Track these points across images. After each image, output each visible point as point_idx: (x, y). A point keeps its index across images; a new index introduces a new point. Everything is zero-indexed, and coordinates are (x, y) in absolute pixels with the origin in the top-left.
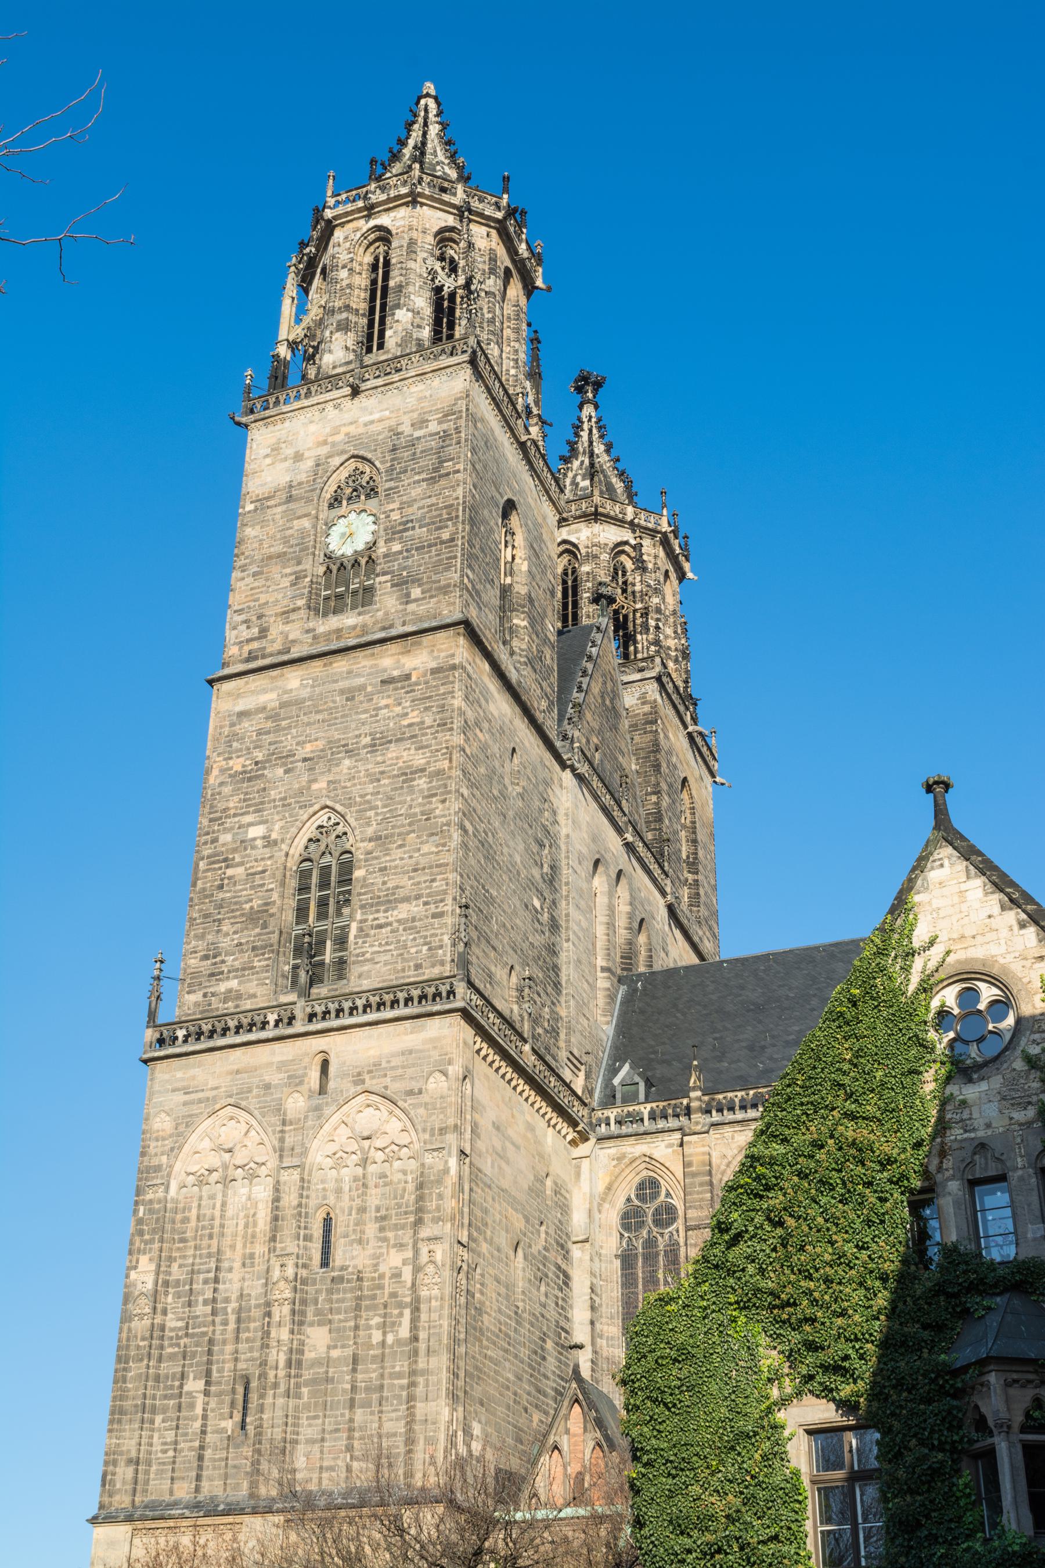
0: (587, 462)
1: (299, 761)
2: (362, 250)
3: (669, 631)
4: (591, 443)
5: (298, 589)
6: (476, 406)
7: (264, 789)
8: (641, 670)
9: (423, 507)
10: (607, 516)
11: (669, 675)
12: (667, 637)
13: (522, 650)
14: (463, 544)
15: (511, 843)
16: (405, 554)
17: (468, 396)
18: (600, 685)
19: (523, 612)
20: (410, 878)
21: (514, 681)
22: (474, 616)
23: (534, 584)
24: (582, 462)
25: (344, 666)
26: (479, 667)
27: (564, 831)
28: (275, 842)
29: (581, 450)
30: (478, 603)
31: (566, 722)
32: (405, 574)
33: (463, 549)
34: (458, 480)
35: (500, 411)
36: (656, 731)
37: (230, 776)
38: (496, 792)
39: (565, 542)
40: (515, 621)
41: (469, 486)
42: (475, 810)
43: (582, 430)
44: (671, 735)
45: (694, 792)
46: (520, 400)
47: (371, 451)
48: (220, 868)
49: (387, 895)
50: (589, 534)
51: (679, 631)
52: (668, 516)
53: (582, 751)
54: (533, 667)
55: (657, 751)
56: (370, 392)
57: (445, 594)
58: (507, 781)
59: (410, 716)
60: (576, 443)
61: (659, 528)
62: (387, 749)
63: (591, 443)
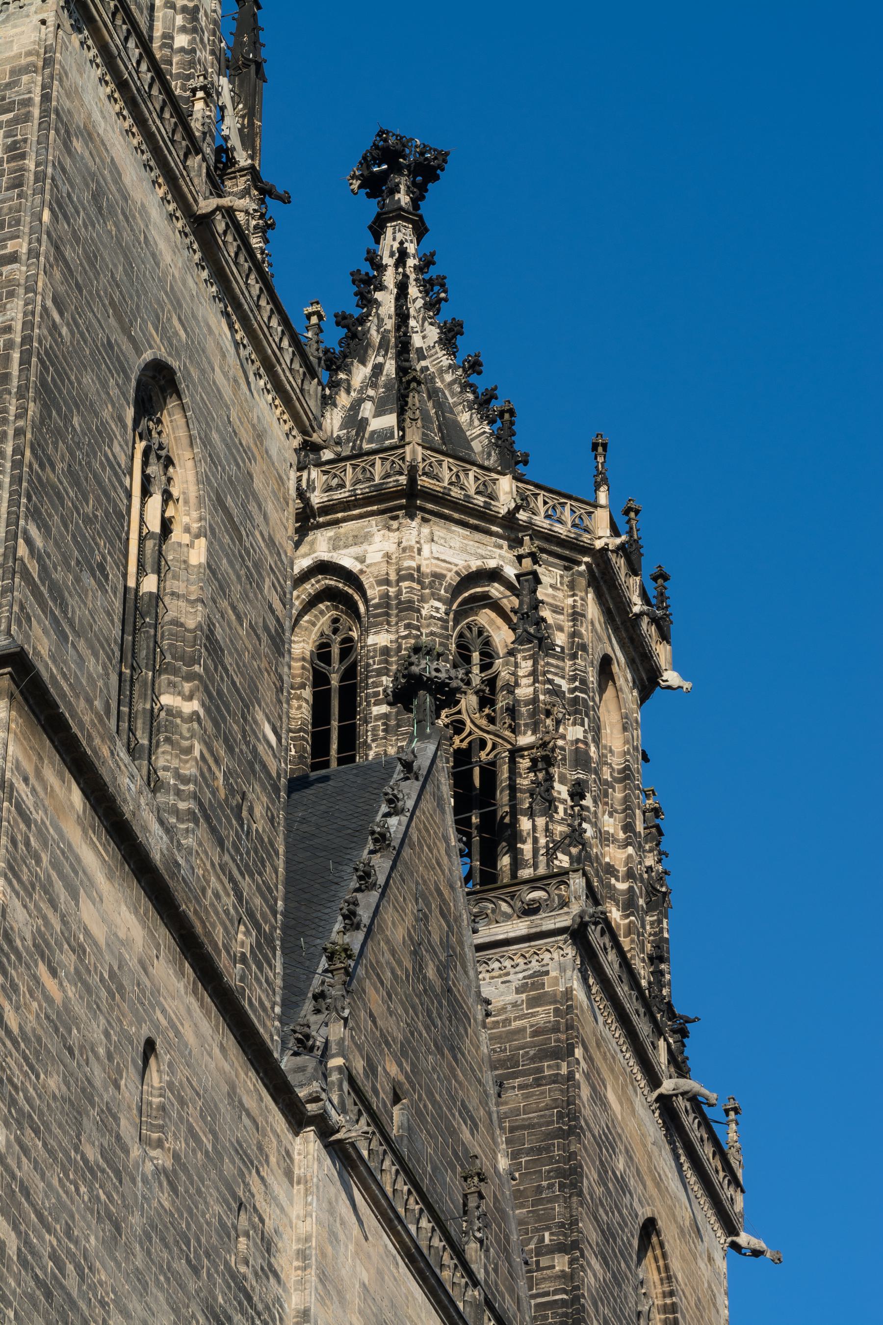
0: (390, 367)
3: (611, 824)
4: (402, 317)
6: (73, 93)
8: (531, 910)
10: (441, 499)
11: (609, 929)
12: (605, 838)
13: (185, 780)
14: (18, 450)
15: (134, 1305)
17: (48, 62)
18: (409, 920)
19: (189, 677)
21: (157, 856)
22: (44, 653)
23: (224, 604)
24: (378, 369)
26: (52, 794)
27: (294, 1302)
29: (375, 337)
30: (55, 621)
31: (309, 1006)
33: (17, 465)
34: (10, 282)
35: (141, 121)
36: (570, 1076)
38: (92, 1153)
39: (323, 568)
40: (166, 699)
41: (43, 299)
42: (26, 1192)
43: (381, 287)
44: (611, 1096)
45: (676, 1265)
46: (199, 106)
50: (391, 548)
51: (639, 827)
52: (611, 507)
53: (352, 1081)
54: (213, 830)
55: (571, 1131)
58: (127, 1129)
60: (362, 320)
61: (586, 538)
63: (402, 317)
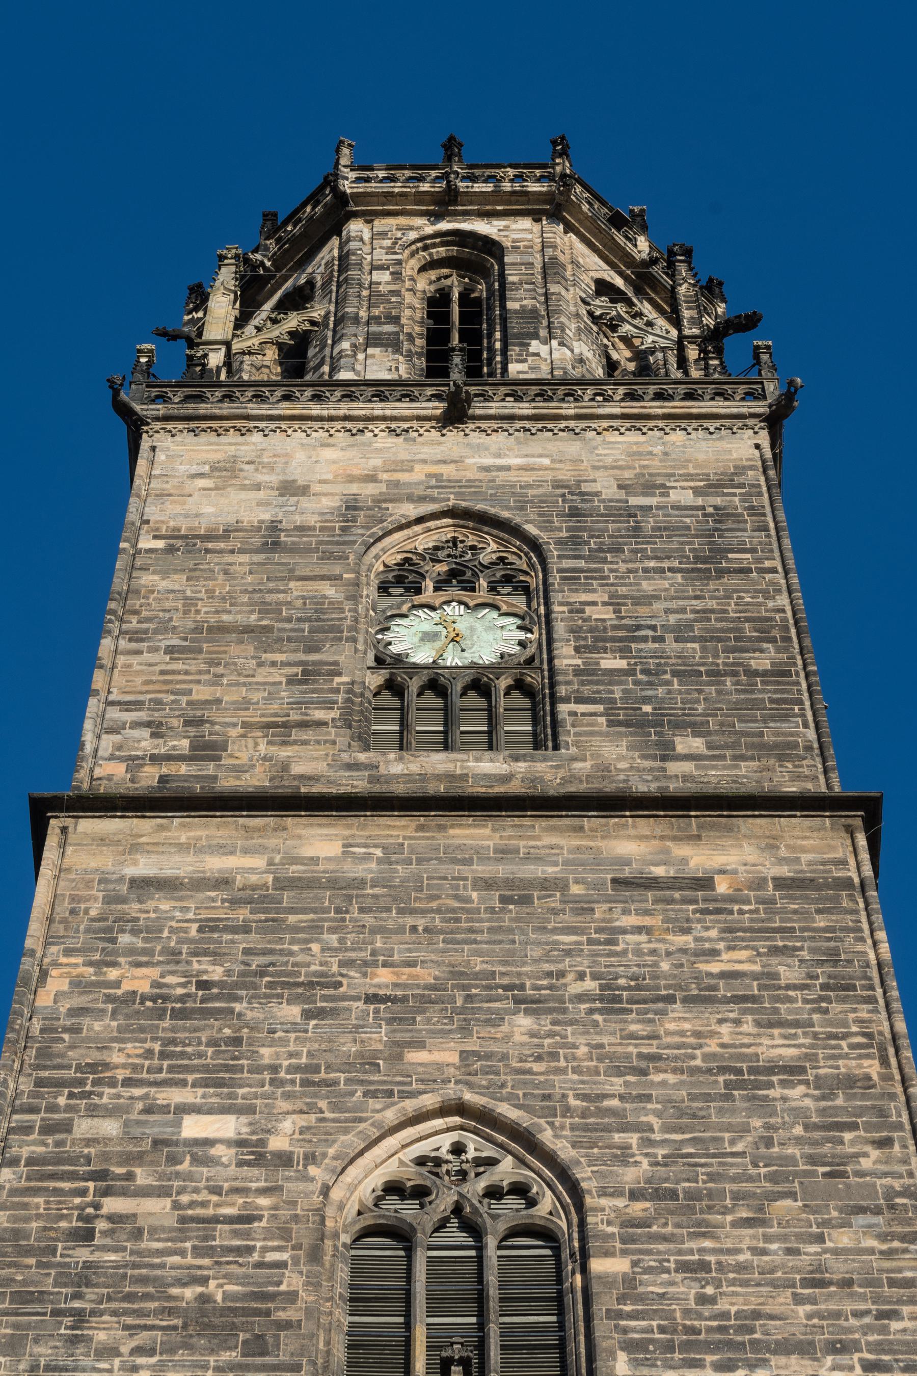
1: (356, 998)
2: (414, 264)
7: (237, 1041)
9: (683, 611)
20: (799, 1300)
25: (489, 838)
28: (285, 1159)
32: (647, 709)
37: (109, 999)
47: (508, 508)
48: (83, 1193)
49: (722, 1329)
56: (494, 425)
57: (781, 758)
59: (725, 956)
62: (664, 1013)
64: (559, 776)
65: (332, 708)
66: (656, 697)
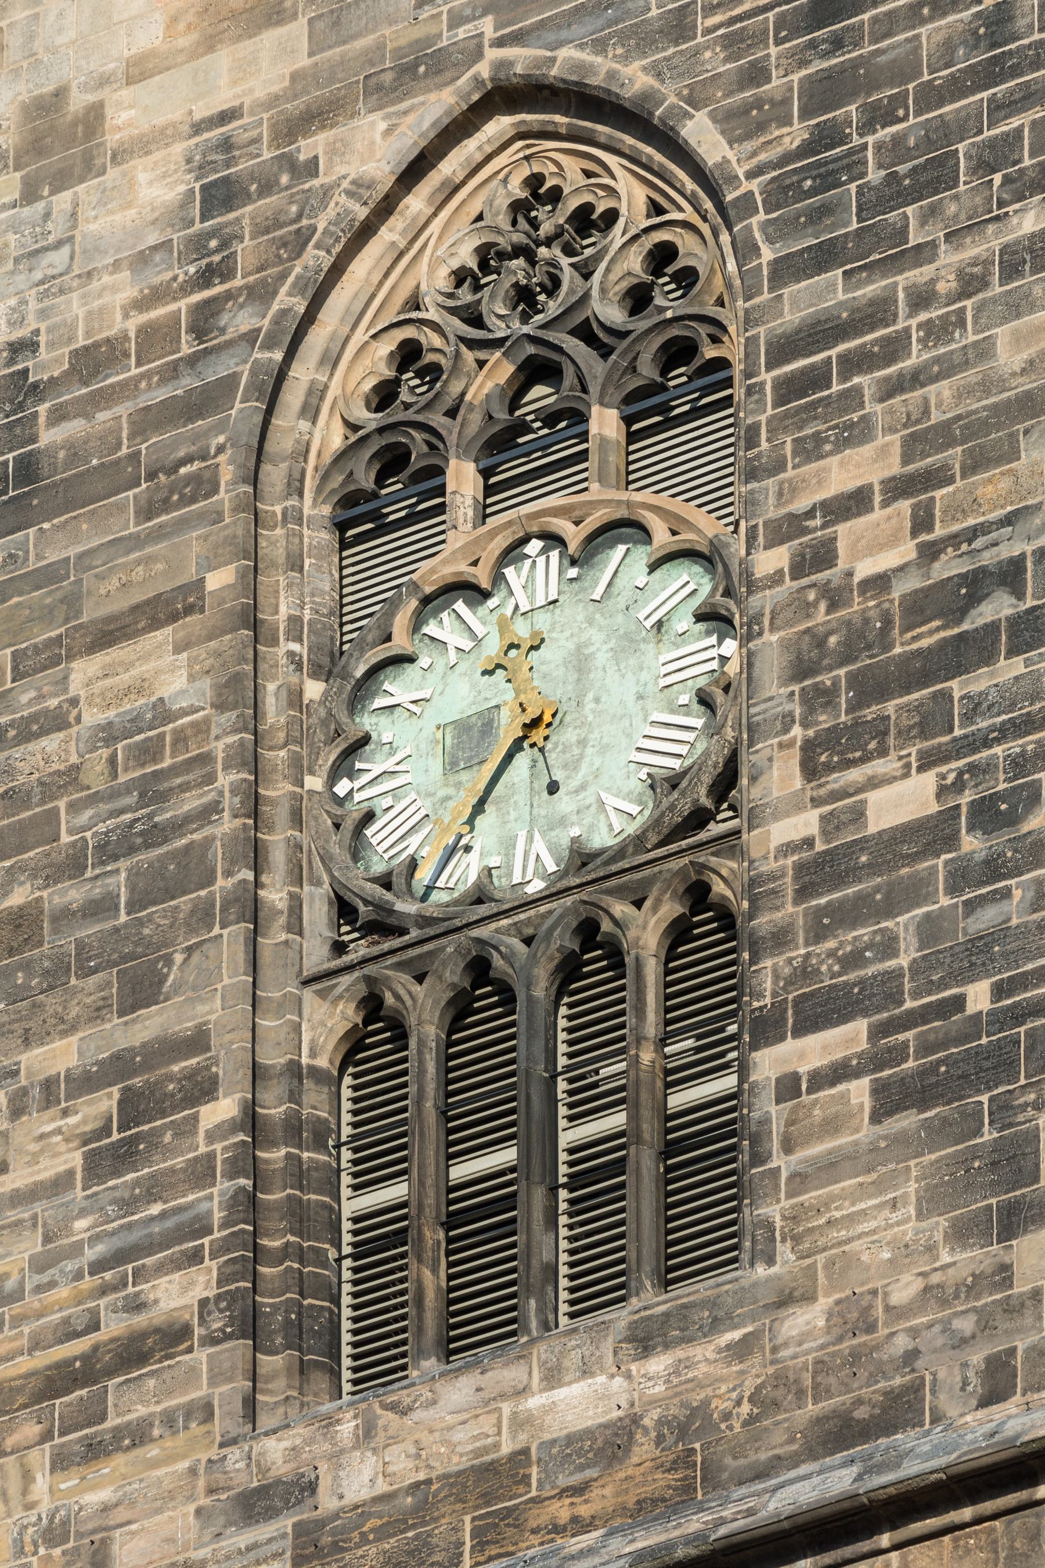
5: (153, 1190)
16: (971, 843)
64: (749, 1385)
65: (195, 1257)
66: (1002, 932)
